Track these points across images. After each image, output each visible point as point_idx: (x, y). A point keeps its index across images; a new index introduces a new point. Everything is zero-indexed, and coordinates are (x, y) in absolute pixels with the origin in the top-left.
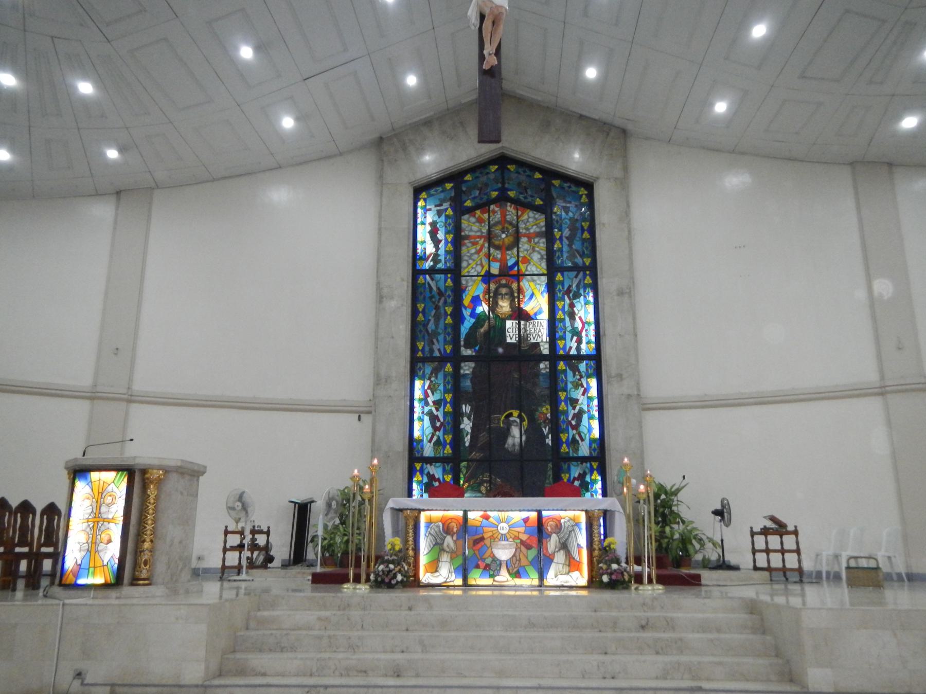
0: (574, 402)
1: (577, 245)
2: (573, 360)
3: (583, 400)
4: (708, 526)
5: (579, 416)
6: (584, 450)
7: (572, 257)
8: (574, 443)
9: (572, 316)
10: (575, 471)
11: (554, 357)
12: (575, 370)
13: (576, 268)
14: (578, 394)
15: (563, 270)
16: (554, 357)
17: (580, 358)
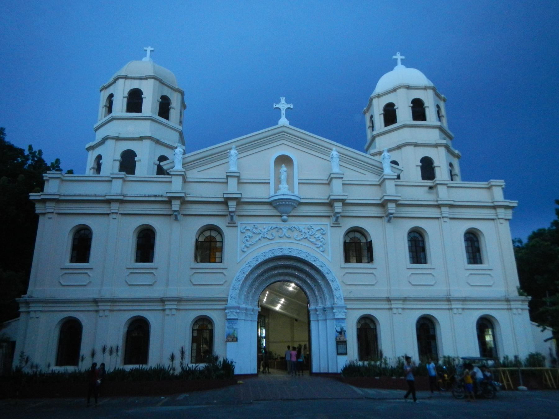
0: (262, 342)
1: (263, 324)
2: (262, 337)
3: (263, 342)
4: (274, 355)
5: (263, 344)
6: (263, 347)
7: (263, 325)
8: (262, 347)
9: (262, 332)
10: (262, 350)
11: (260, 337)
12: (262, 338)
13: (263, 327)
14: (263, 341)
15: (261, 327)
16: (260, 337)
17: (263, 337)
